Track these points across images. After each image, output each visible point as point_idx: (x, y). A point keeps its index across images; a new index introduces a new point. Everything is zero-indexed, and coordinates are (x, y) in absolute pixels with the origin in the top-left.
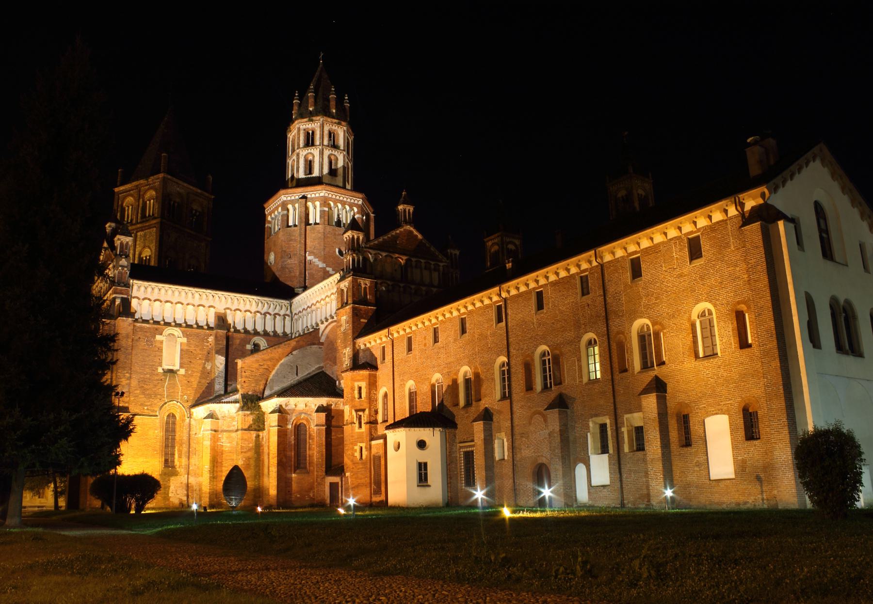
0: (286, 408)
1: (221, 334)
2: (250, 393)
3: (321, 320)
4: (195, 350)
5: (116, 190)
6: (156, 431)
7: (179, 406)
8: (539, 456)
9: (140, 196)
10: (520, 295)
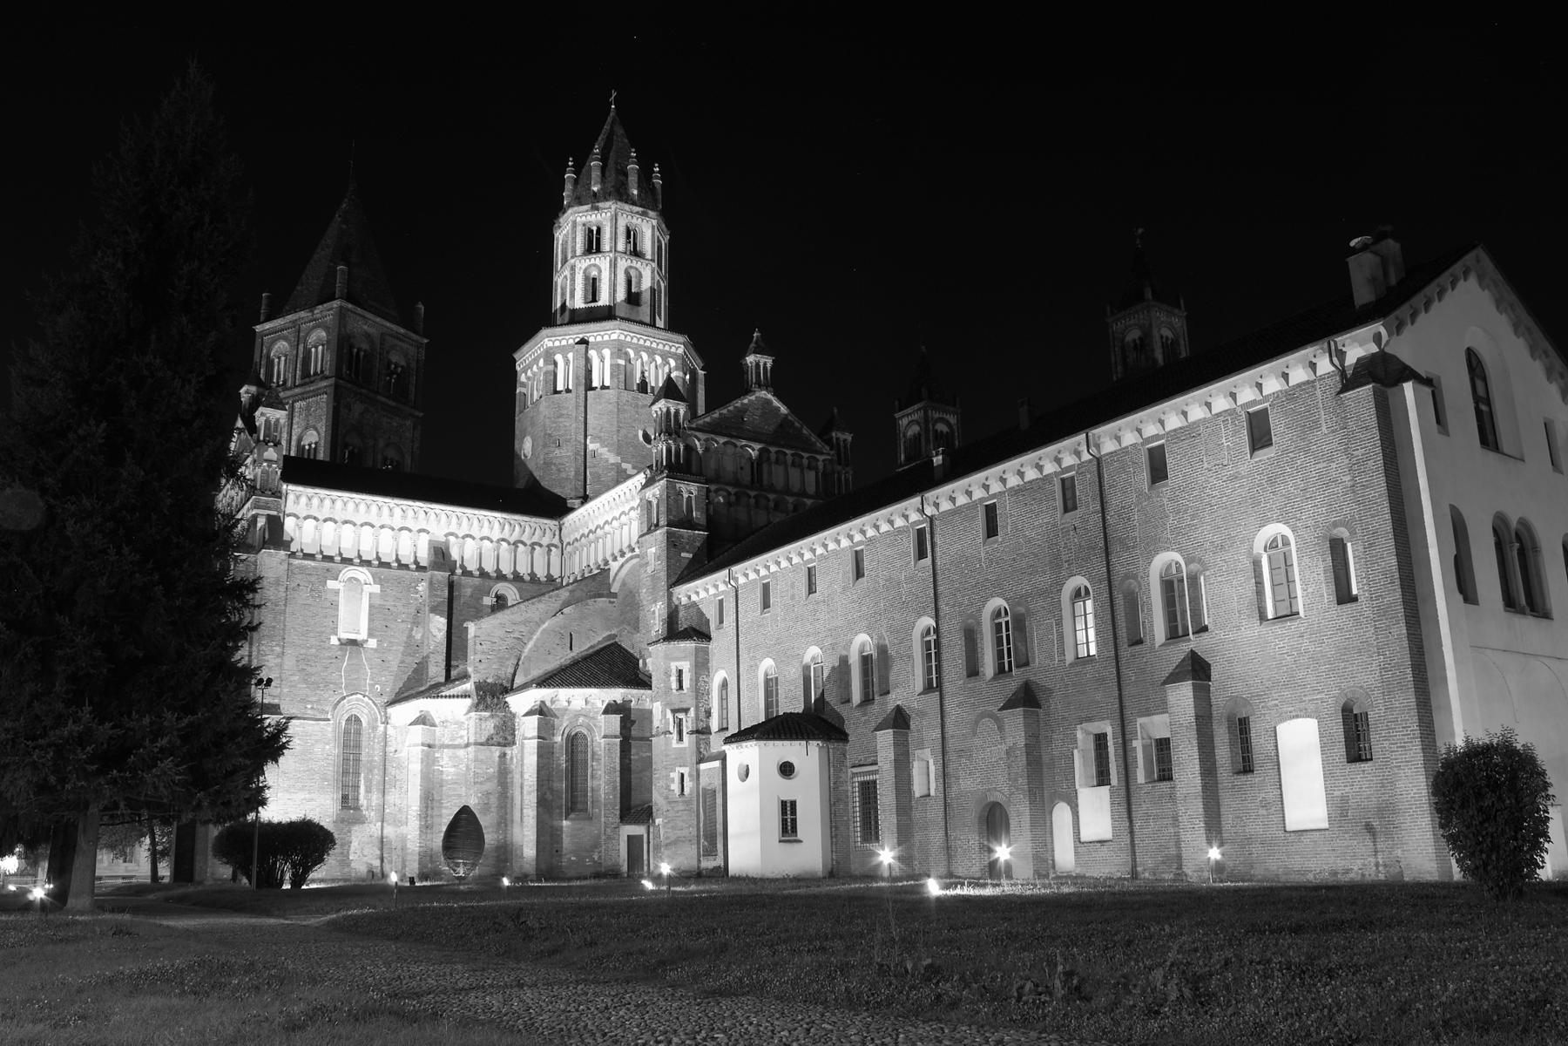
0: (553, 707)
1: (440, 578)
2: (489, 681)
3: (613, 554)
5: (258, 328)
6: (327, 747)
7: (367, 704)
8: (989, 790)
9: (299, 339)
10: (956, 512)
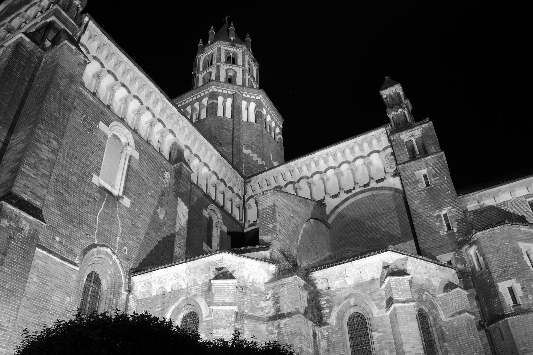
4: (147, 178)
6: (68, 299)
7: (114, 263)
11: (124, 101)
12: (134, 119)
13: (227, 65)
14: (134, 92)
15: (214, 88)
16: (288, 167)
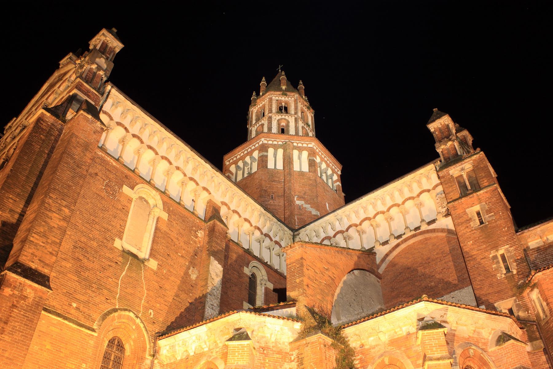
4: (178, 239)
6: (84, 365)
7: (138, 327)
11: (152, 163)
12: (164, 180)
13: (278, 115)
14: (162, 152)
15: (263, 141)
16: (336, 216)
